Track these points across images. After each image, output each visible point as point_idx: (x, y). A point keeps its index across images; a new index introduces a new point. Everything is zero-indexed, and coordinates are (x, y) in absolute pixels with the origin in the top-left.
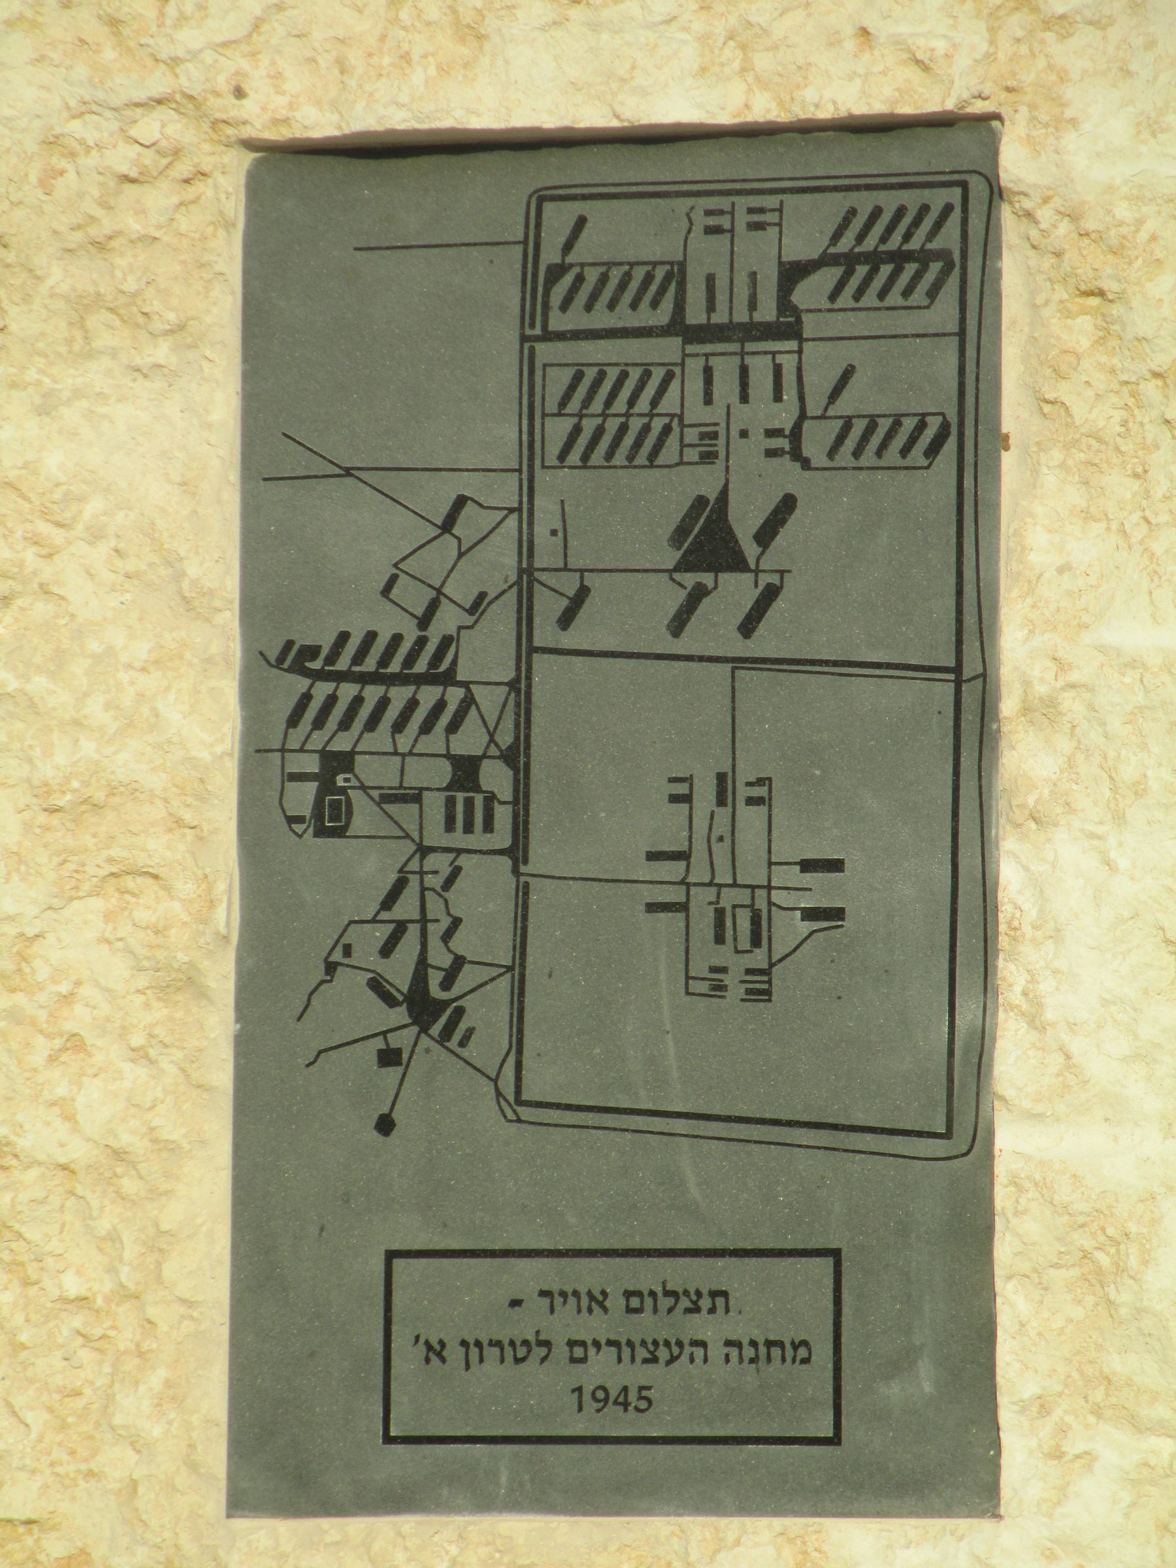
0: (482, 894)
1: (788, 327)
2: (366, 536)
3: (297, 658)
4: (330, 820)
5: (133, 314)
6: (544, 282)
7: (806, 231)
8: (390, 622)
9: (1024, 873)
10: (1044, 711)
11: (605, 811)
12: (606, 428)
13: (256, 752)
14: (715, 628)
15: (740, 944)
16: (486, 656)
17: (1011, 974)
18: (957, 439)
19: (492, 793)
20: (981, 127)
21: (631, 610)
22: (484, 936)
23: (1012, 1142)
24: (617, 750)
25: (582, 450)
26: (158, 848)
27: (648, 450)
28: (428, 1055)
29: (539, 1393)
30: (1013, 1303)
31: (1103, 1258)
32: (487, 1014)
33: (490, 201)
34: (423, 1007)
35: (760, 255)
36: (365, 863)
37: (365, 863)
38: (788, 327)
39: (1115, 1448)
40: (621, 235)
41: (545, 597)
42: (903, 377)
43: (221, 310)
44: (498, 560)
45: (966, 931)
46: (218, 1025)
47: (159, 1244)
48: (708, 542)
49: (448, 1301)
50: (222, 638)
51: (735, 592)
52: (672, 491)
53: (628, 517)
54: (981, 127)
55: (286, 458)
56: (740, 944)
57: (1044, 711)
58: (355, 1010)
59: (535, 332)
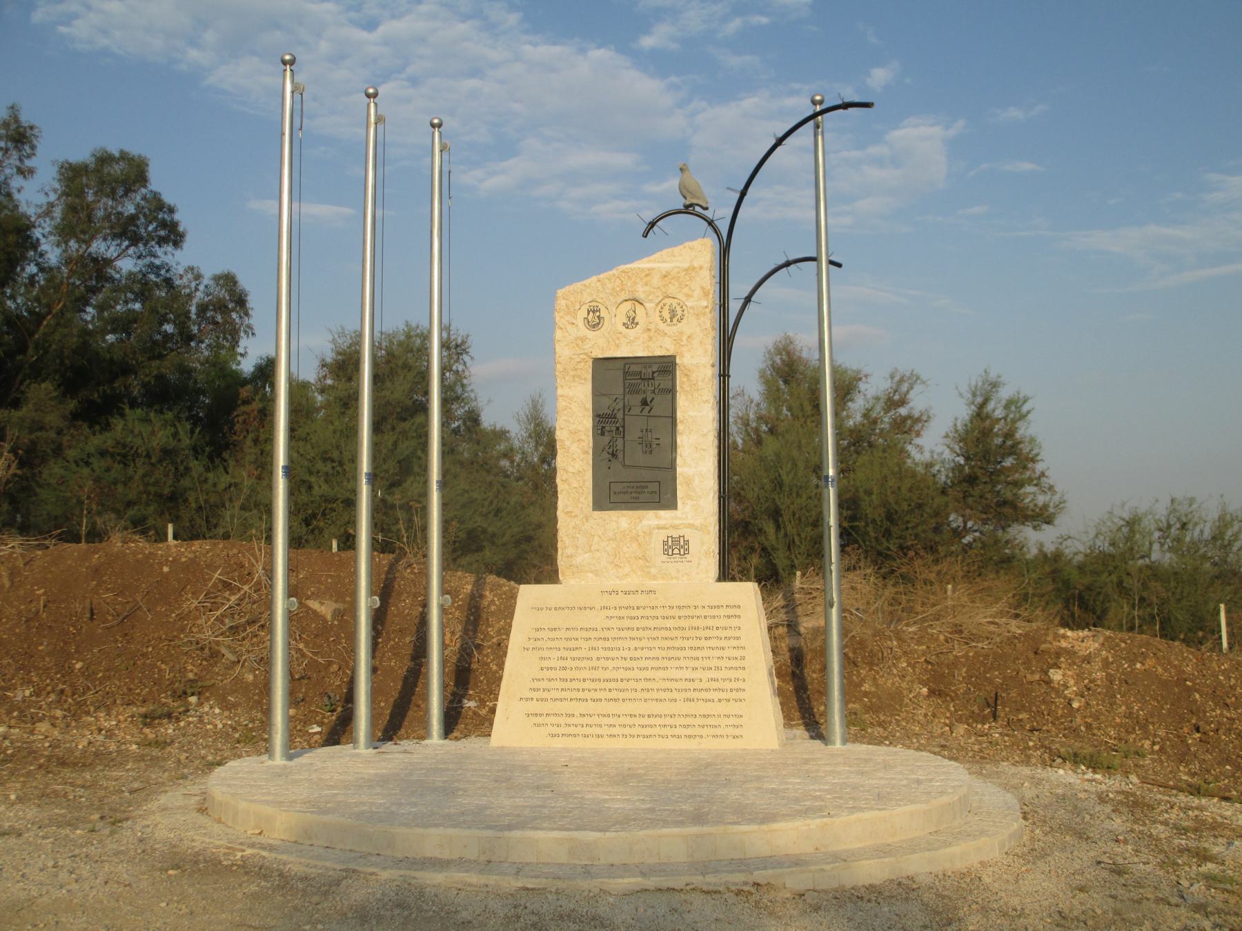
0: (620, 442)
1: (653, 378)
2: (606, 402)
3: (599, 416)
4: (603, 434)
5: (579, 377)
6: (626, 373)
7: (655, 368)
8: (609, 412)
9: (681, 440)
10: (682, 422)
11: (633, 434)
12: (633, 390)
13: (594, 427)
14: (646, 412)
15: (648, 448)
16: (620, 415)
17: (679, 451)
18: (672, 391)
19: (621, 431)
20: (674, 357)
21: (636, 410)
22: (620, 447)
23: (679, 470)
24: (635, 427)
25: (630, 392)
26: (583, 437)
27: (638, 392)
28: (613, 460)
29: (627, 497)
30: (679, 487)
31: (688, 483)
32: (620, 455)
33: (622, 363)
34: (613, 455)
35: (650, 371)
36: (607, 439)
37: (607, 439)
38: (653, 378)
39: (689, 502)
40: (634, 368)
41: (626, 409)
42: (668, 385)
43: (590, 377)
44: (621, 405)
45: (673, 446)
46: (590, 457)
47: (584, 481)
48: (644, 403)
49: (617, 487)
50: (590, 413)
51: (647, 408)
52: (640, 397)
53: (636, 400)
54: (674, 357)
55: (597, 393)
56: (648, 448)
57: (682, 422)
58: (606, 455)
59: (625, 379)
